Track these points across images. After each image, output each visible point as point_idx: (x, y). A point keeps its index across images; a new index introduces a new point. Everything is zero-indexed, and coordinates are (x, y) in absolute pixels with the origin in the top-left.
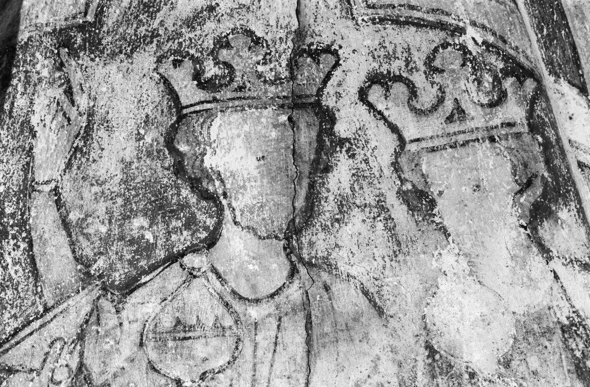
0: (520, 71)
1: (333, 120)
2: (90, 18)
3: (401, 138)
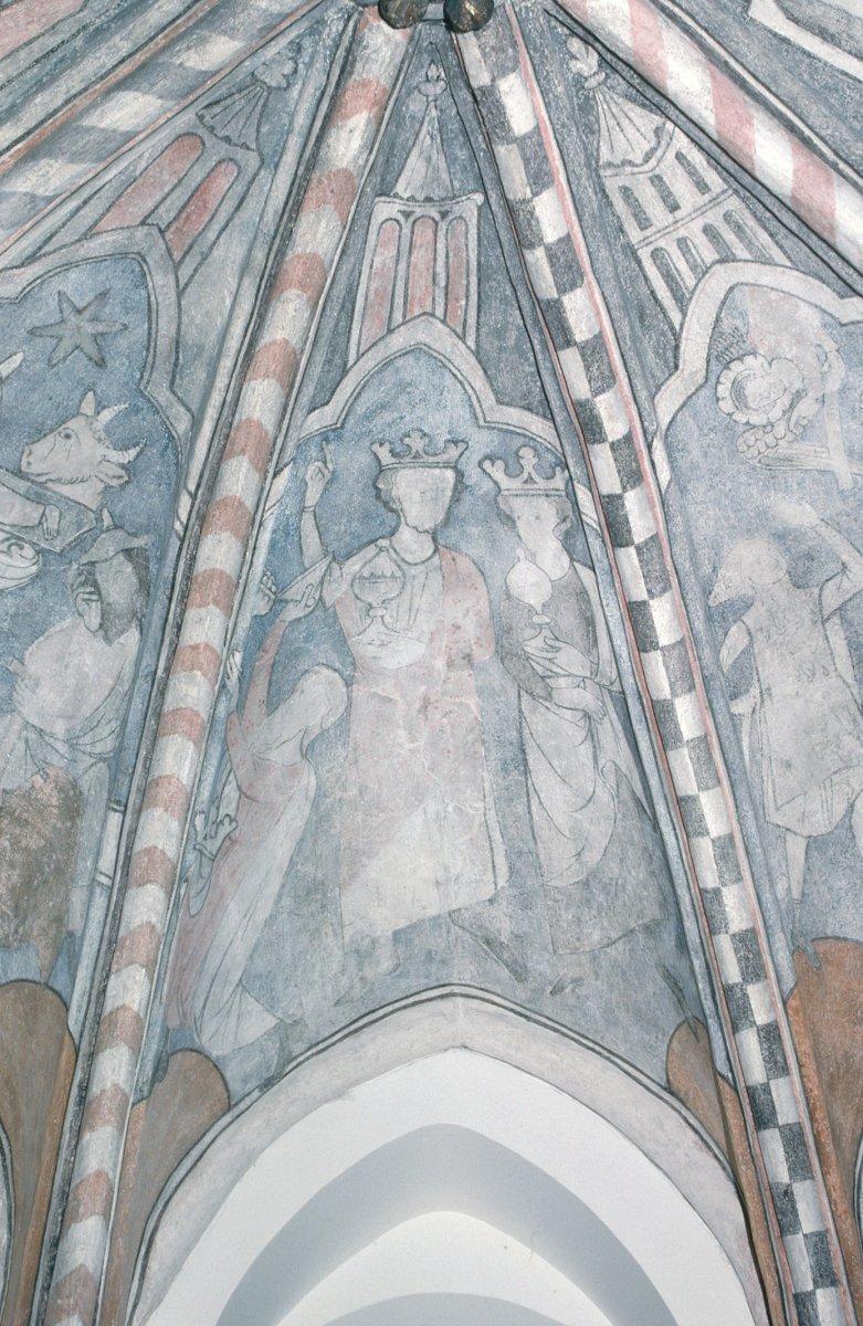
1: (463, 476)
2: (338, 425)
3: (499, 487)
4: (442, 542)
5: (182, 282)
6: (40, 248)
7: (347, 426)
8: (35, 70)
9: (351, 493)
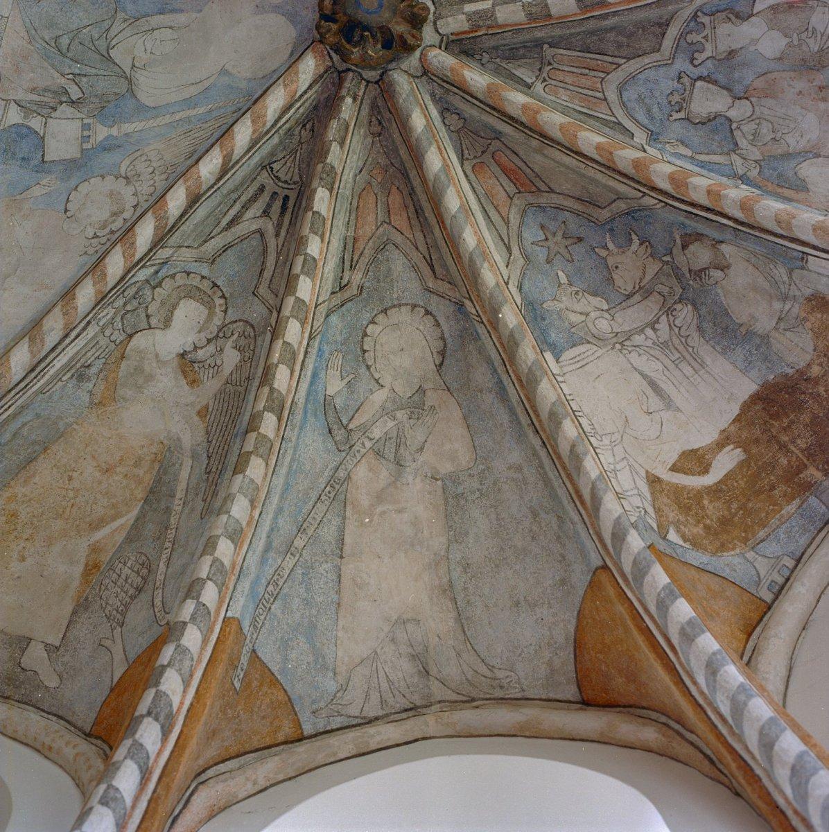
0: (695, 16)
4: (742, 94)
5: (548, 190)
6: (505, 244)
7: (653, 129)
8: (422, 220)
9: (695, 136)
